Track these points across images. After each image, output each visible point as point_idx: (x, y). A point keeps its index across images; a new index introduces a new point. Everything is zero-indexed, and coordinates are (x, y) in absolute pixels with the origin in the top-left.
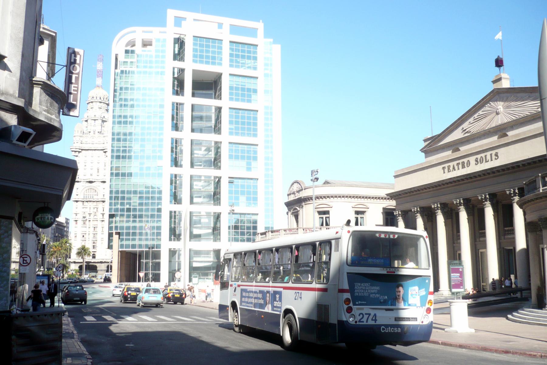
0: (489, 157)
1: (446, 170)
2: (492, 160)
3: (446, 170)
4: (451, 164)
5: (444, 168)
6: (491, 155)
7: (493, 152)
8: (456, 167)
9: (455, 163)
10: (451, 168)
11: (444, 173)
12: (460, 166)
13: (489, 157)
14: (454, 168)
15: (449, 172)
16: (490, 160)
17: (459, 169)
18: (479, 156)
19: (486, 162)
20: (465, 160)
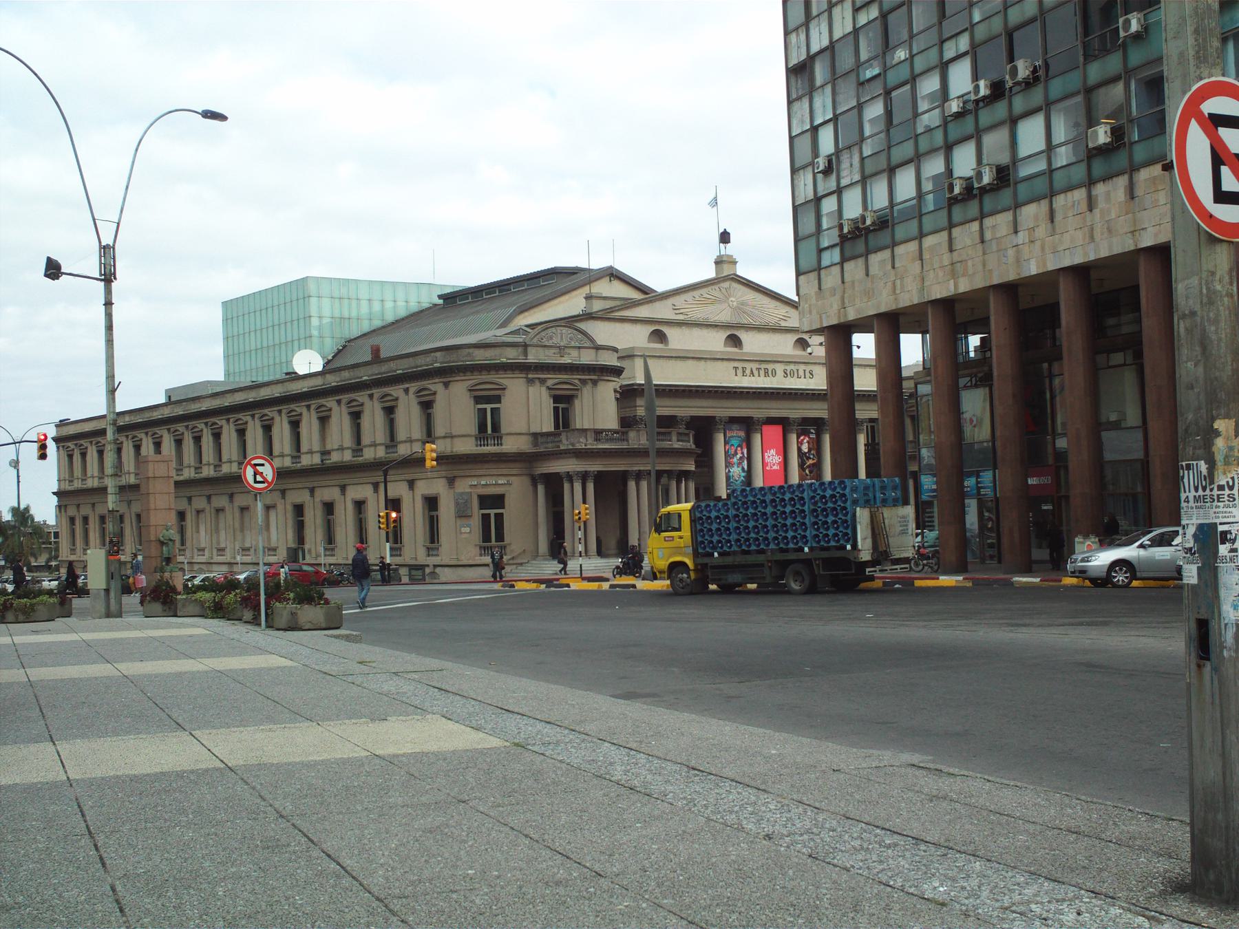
1: (740, 372)
3: (740, 372)
4: (749, 366)
5: (736, 368)
7: (809, 368)
8: (756, 373)
9: (754, 366)
10: (748, 372)
12: (762, 372)
18: (789, 368)
20: (770, 367)
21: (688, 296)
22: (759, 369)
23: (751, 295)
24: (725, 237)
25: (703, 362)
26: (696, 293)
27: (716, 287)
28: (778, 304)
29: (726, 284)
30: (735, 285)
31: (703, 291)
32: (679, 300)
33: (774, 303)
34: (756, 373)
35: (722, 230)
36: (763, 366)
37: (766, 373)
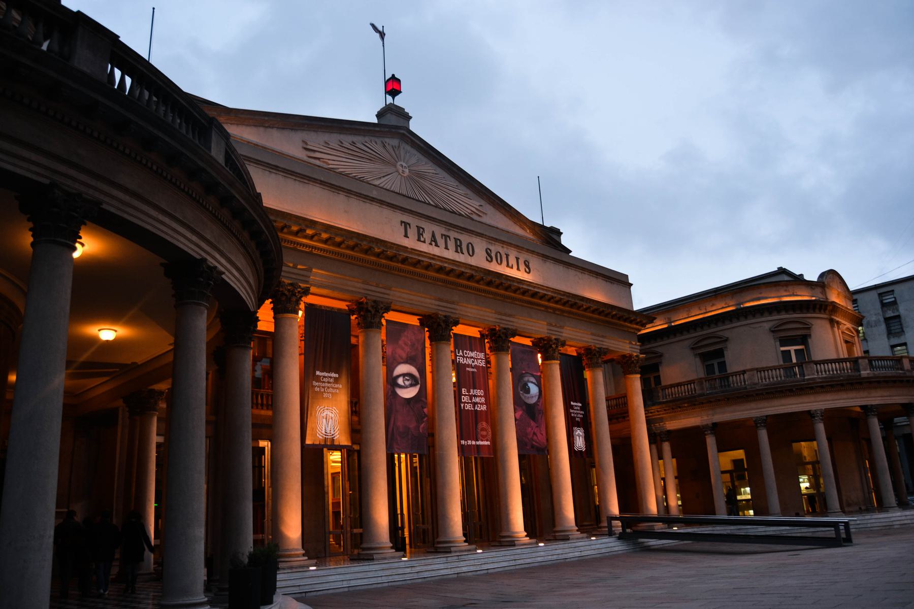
0: (512, 261)
1: (412, 232)
2: (518, 269)
3: (412, 232)
4: (429, 228)
5: (406, 225)
6: (517, 259)
9: (439, 230)
10: (427, 236)
11: (406, 236)
12: (451, 244)
13: (512, 261)
14: (434, 240)
15: (419, 240)
16: (515, 267)
17: (446, 248)
18: (495, 248)
19: (508, 266)
20: (465, 239)
21: (333, 139)
22: (446, 237)
23: (428, 168)
24: (393, 87)
25: (342, 197)
26: (347, 139)
27: (379, 141)
28: (469, 192)
29: (395, 142)
30: (408, 148)
31: (358, 139)
32: (316, 140)
33: (463, 190)
34: (441, 242)
35: (388, 76)
36: (453, 234)
37: (458, 248)
